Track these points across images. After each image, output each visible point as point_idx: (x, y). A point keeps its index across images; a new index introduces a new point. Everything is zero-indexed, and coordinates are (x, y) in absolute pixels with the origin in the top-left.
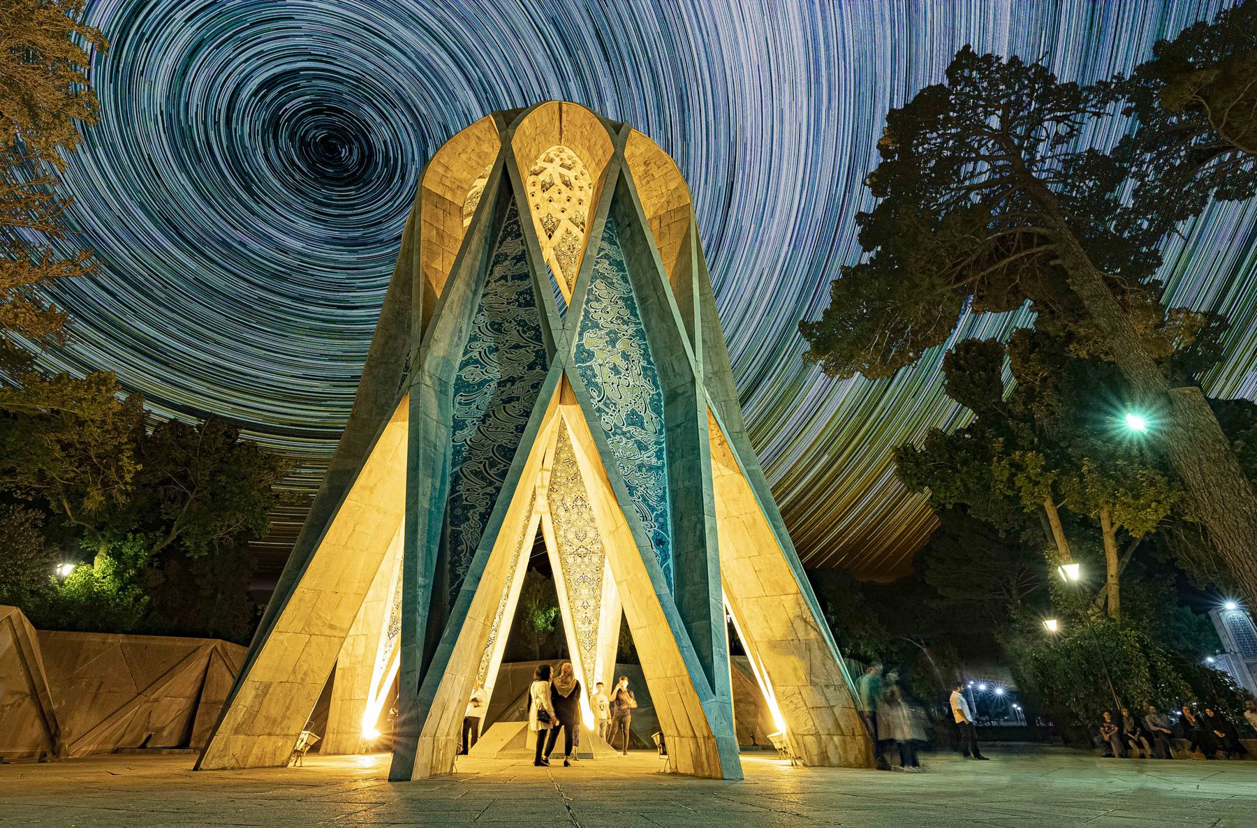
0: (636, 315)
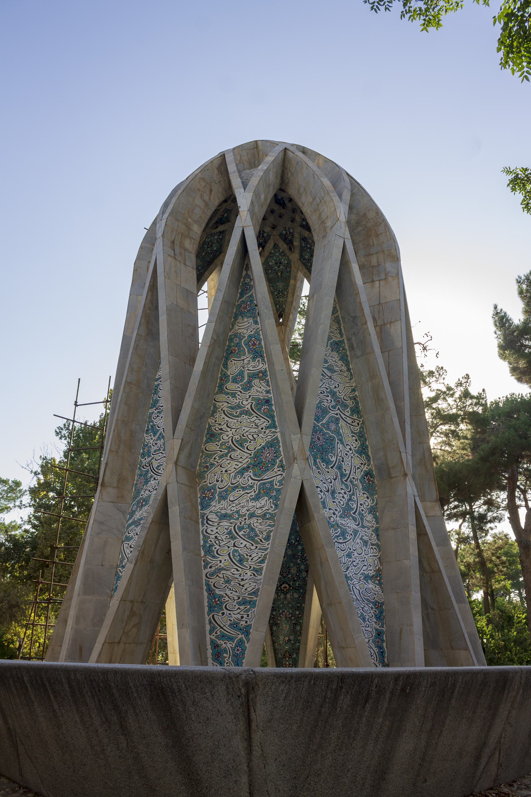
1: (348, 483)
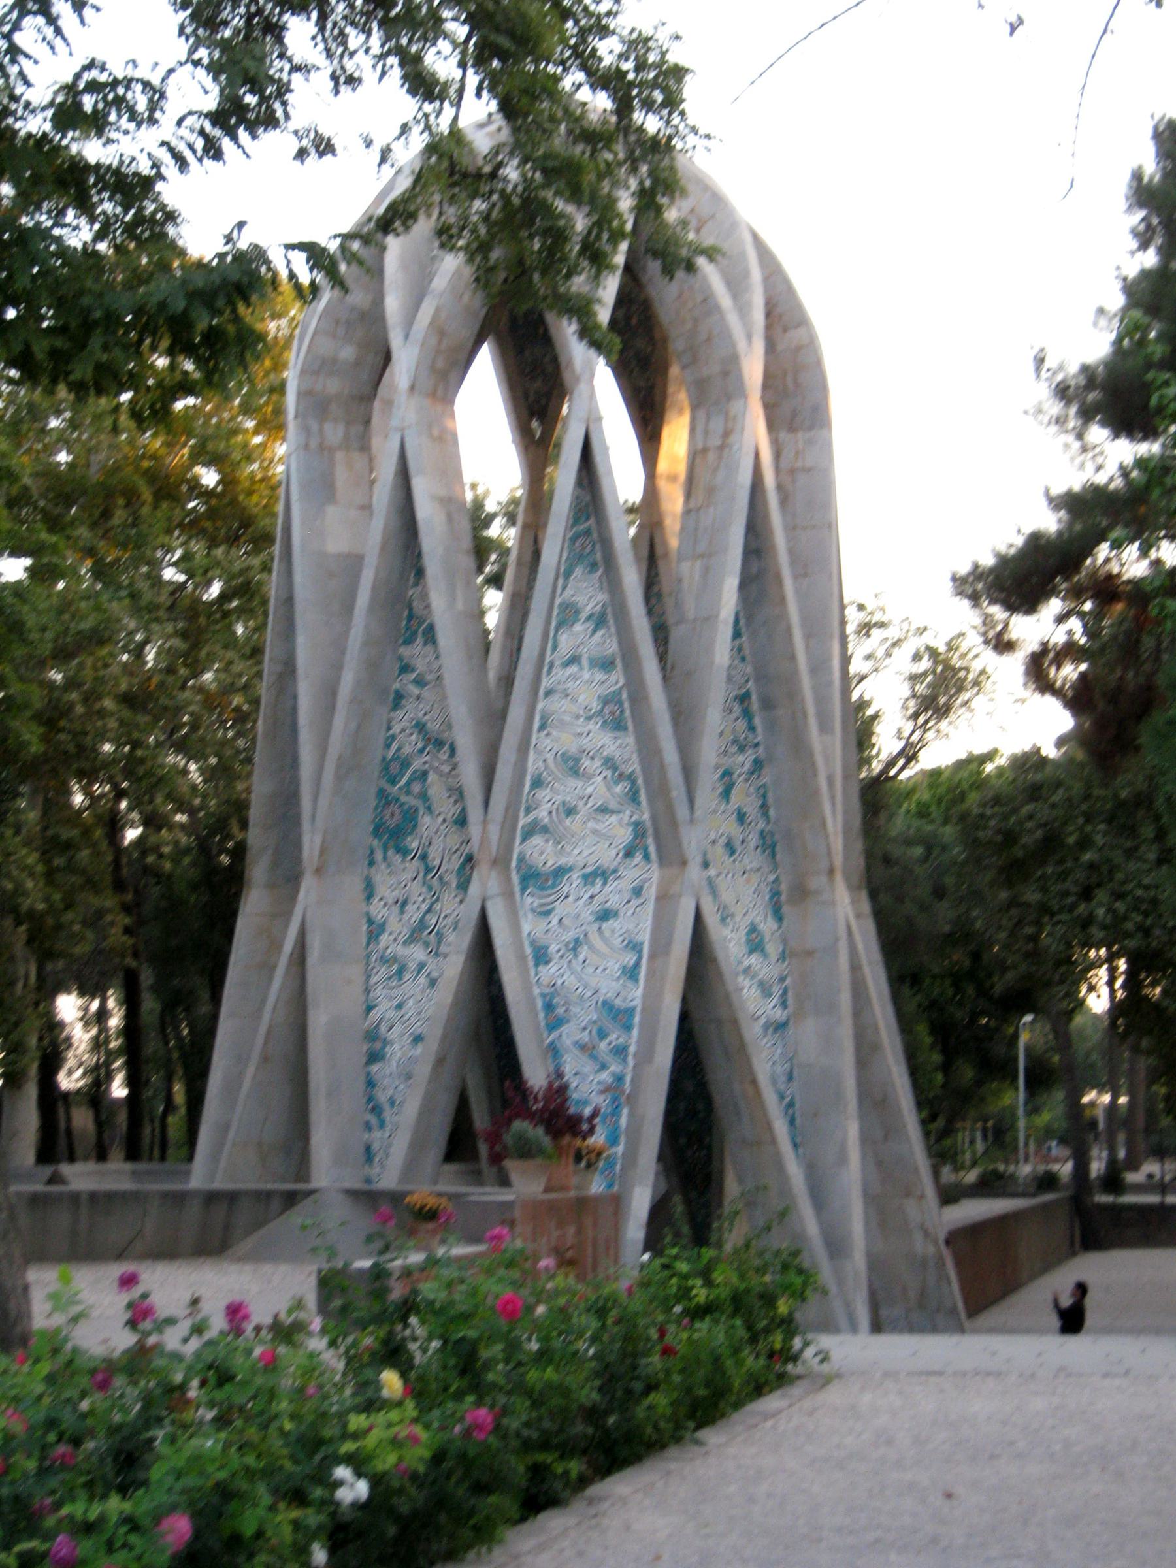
0: (752, 728)
1: (435, 881)
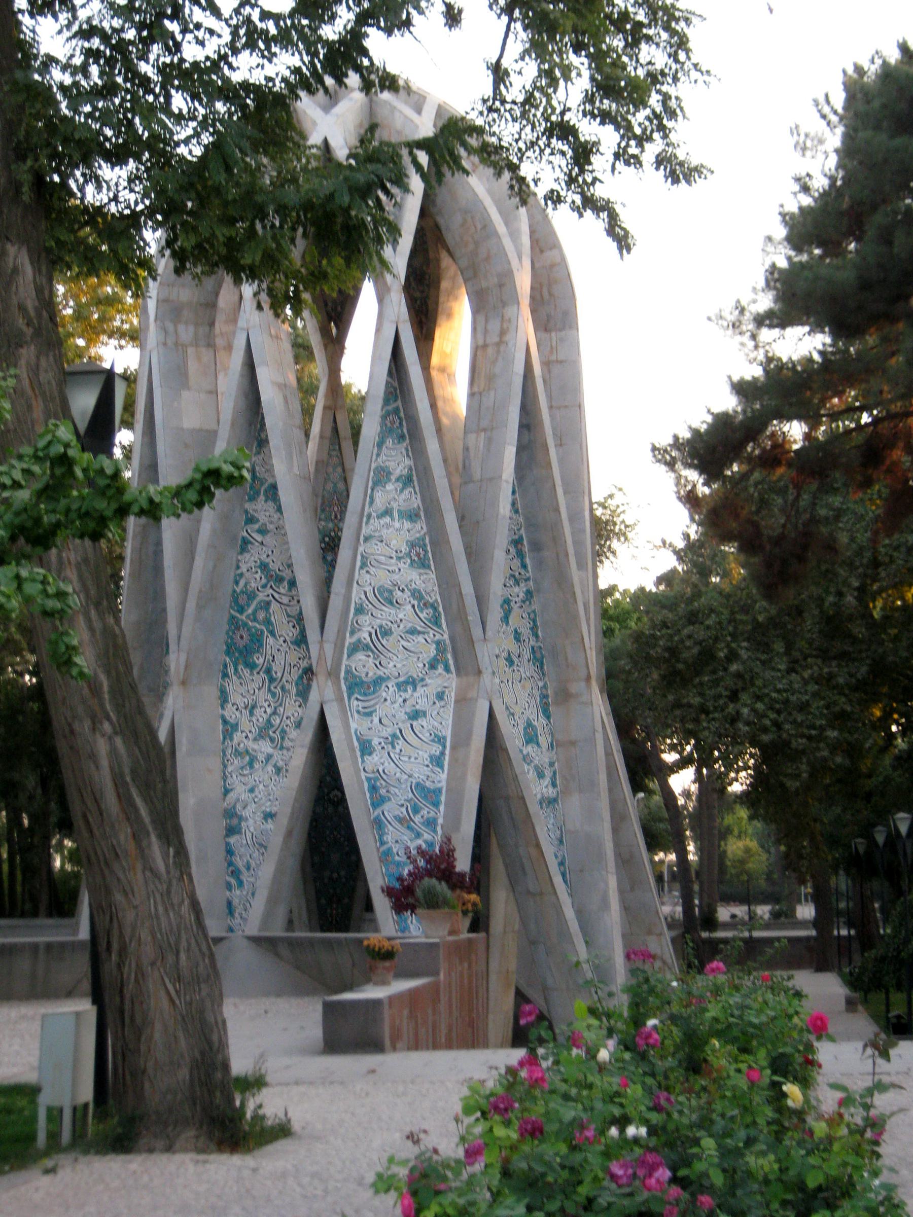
0: (524, 566)
1: (278, 691)
